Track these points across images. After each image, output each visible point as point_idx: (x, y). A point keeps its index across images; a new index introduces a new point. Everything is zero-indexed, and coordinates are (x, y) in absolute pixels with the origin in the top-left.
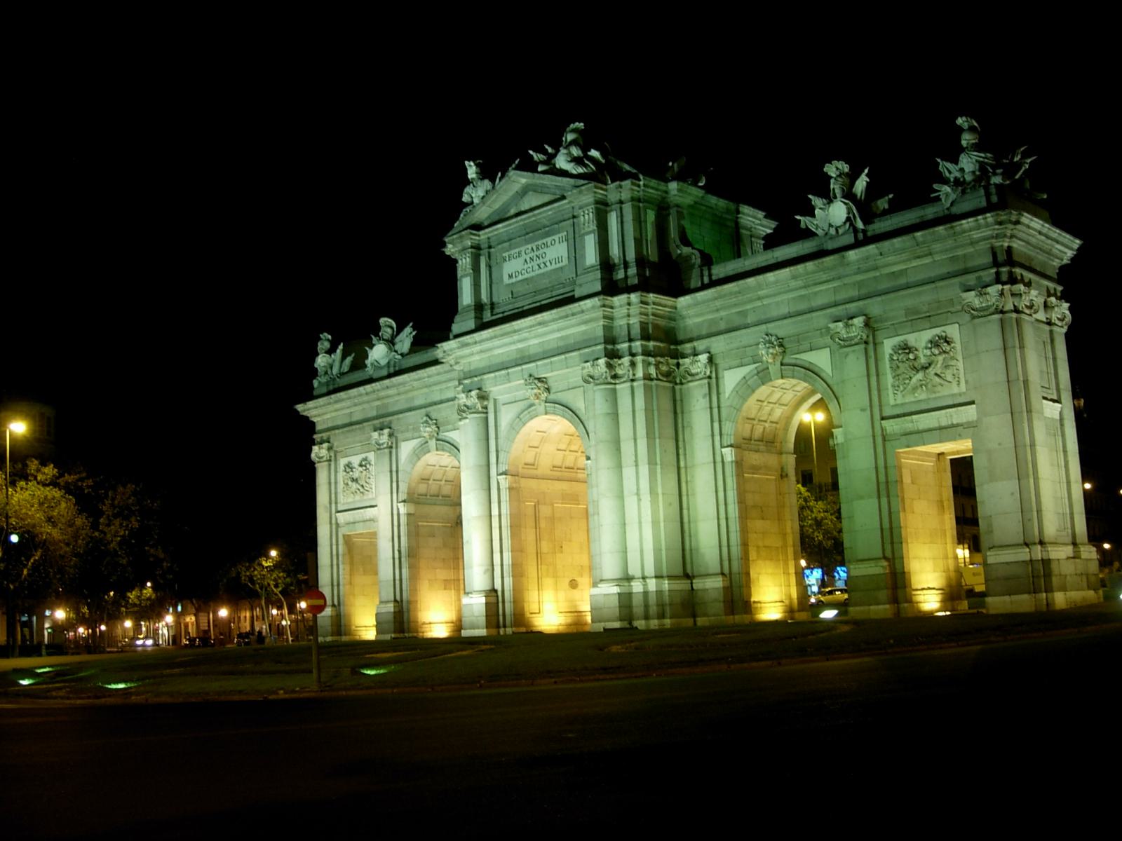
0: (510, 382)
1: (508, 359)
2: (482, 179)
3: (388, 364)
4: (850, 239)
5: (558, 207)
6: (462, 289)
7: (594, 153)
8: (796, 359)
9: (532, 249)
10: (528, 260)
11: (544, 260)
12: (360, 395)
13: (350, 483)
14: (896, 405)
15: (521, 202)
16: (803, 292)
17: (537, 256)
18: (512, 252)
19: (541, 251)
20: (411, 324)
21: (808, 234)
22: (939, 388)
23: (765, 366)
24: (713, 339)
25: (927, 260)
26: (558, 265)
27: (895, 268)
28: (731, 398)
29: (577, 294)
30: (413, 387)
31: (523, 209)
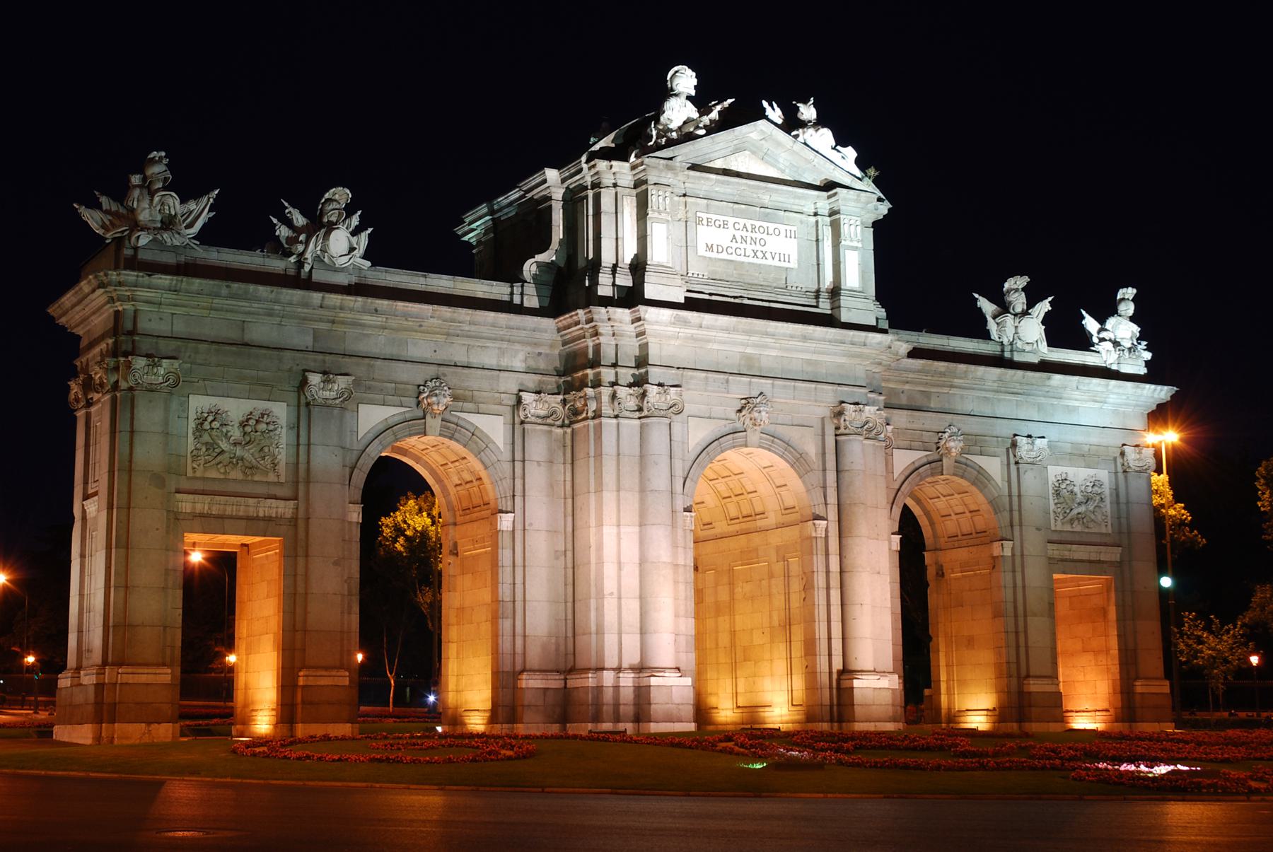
0: (728, 393)
2: (689, 98)
7: (850, 153)
9: (745, 226)
10: (739, 239)
11: (764, 249)
12: (306, 305)
14: (1055, 531)
18: (714, 217)
19: (758, 236)
20: (359, 212)
21: (986, 336)
22: (1091, 525)
23: (936, 457)
25: (1097, 405)
29: (845, 317)
30: (421, 326)
31: (734, 168)
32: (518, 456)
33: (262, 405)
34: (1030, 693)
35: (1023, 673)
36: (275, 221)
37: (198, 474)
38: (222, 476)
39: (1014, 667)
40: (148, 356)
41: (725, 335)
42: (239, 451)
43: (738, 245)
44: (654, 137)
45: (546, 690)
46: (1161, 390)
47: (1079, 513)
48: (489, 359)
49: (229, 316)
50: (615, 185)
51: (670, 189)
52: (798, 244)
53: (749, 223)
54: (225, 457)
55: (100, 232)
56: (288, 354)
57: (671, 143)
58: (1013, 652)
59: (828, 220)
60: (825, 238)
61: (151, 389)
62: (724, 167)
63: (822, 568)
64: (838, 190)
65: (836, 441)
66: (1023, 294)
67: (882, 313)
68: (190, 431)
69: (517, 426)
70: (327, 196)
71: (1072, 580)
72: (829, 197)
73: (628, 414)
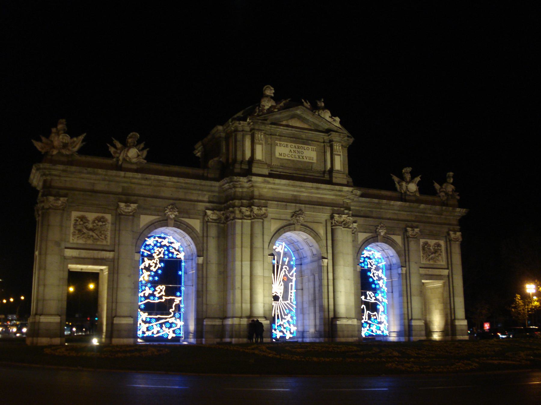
0: (286, 210)
1: (286, 197)
2: (272, 97)
3: (136, 163)
4: (413, 198)
5: (318, 135)
6: (335, 165)
7: (338, 119)
8: (388, 236)
9: (295, 146)
11: (303, 155)
12: (119, 176)
13: (85, 231)
14: (423, 264)
15: (290, 121)
16: (397, 212)
17: (298, 151)
18: (282, 143)
19: (300, 150)
20: (144, 142)
21: (395, 190)
22: (437, 261)
23: (376, 235)
24: (359, 218)
25: (439, 216)
26: (310, 161)
27: (429, 215)
28: (361, 245)
30: (165, 185)
32: (205, 234)
33: (100, 215)
34: (412, 325)
35: (410, 318)
36: (109, 145)
37: (75, 241)
38: (84, 242)
39: (406, 316)
40: (55, 196)
41: (285, 188)
42: (91, 233)
43: (293, 154)
44: (257, 112)
45: (214, 325)
46: (463, 210)
47: (432, 257)
48: (194, 198)
49: (88, 181)
50: (243, 131)
51: (264, 132)
52: (317, 153)
53: (297, 145)
54: (86, 236)
55: (40, 150)
56: (111, 195)
57: (264, 114)
58: (406, 310)
59: (329, 144)
60: (328, 151)
61: (56, 208)
62: (287, 124)
63: (326, 278)
64: (332, 132)
65: (332, 229)
66: (410, 174)
67: (350, 180)
68: (72, 225)
69: (205, 223)
70: (129, 135)
71: (431, 282)
72: (328, 136)
73: (246, 218)
